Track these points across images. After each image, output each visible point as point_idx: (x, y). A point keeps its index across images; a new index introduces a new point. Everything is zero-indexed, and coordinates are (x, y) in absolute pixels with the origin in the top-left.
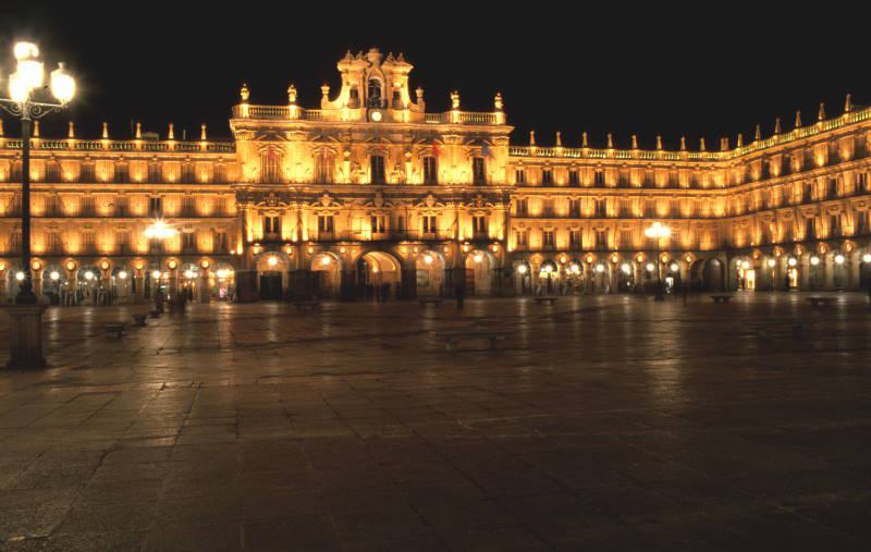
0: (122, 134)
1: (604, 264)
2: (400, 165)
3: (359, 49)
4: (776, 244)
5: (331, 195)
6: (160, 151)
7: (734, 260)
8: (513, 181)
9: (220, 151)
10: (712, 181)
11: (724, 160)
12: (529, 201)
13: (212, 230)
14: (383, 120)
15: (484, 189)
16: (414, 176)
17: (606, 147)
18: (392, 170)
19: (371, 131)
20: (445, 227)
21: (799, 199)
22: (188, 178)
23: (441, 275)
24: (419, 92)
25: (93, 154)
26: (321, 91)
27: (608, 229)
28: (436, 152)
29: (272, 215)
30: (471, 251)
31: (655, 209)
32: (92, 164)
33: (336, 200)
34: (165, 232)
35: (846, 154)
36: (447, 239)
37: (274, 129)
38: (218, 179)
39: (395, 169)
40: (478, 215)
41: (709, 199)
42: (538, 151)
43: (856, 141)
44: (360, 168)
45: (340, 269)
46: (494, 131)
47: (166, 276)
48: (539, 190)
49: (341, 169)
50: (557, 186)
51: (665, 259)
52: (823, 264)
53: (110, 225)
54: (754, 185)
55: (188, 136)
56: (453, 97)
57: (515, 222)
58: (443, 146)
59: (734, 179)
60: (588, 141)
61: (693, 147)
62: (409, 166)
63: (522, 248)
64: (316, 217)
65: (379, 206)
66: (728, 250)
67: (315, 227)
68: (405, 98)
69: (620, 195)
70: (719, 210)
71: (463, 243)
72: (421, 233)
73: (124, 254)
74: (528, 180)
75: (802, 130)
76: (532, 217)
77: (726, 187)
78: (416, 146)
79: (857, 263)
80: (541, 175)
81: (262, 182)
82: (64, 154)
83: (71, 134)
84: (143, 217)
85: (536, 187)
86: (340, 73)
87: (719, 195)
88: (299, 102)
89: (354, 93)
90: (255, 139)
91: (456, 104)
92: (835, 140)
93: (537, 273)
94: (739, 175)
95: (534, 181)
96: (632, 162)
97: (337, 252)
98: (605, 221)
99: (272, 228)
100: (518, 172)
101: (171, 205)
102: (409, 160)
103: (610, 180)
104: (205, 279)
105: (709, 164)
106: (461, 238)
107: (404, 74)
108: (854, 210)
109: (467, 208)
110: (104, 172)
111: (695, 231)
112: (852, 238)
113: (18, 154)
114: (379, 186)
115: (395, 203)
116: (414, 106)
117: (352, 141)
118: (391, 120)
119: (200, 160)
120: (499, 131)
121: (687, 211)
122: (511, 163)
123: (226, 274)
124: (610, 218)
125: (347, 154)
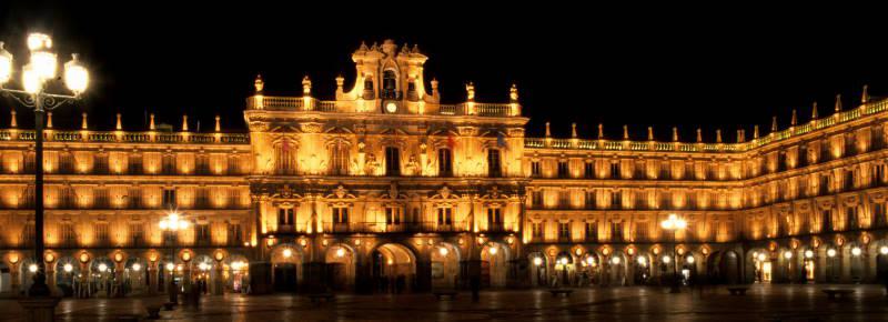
0: (135, 126)
1: (621, 257)
2: (415, 157)
3: (374, 40)
4: (792, 236)
5: (346, 187)
6: (174, 142)
7: (750, 252)
8: (528, 172)
9: (234, 143)
10: (728, 173)
11: (741, 152)
12: (545, 192)
13: (226, 222)
14: (397, 112)
15: (500, 181)
16: (429, 168)
17: (622, 139)
18: (407, 162)
19: (386, 122)
20: (460, 218)
21: (815, 191)
22: (202, 170)
23: (456, 267)
24: (434, 83)
25: (106, 146)
27: (623, 221)
28: (451, 144)
29: (287, 207)
30: (486, 243)
31: (671, 201)
32: (105, 155)
33: (350, 192)
34: (177, 223)
35: (863, 146)
36: (462, 231)
37: (289, 120)
38: (232, 171)
39: (410, 161)
40: (493, 207)
41: (725, 190)
42: (553, 143)
43: (873, 132)
45: (354, 261)
46: (510, 122)
47: (180, 268)
48: (554, 182)
49: (355, 161)
50: (573, 178)
51: (681, 251)
52: (840, 257)
53: (124, 218)
54: (770, 177)
55: (202, 128)
56: (468, 88)
57: (530, 214)
58: (458, 138)
59: (750, 171)
60: (604, 133)
61: (709, 138)
62: (424, 157)
63: (537, 240)
64: (331, 208)
65: (393, 198)
66: (745, 242)
67: (329, 219)
68: (420, 89)
69: (638, 187)
70: (736, 202)
71: (478, 235)
72: (436, 226)
73: (138, 246)
74: (543, 172)
75: (819, 122)
76: (547, 209)
77: (743, 179)
78: (431, 137)
79: (874, 256)
80: (556, 167)
81: (277, 174)
82: (78, 145)
83: (85, 126)
84: (157, 208)
85: (553, 178)
87: (735, 187)
88: (312, 94)
89: (369, 84)
90: (269, 130)
91: (471, 95)
92: (852, 132)
93: (552, 265)
94: (755, 166)
95: (549, 173)
96: (647, 154)
97: (352, 244)
98: (621, 213)
99: (287, 219)
100: (533, 164)
101: (185, 197)
102: (424, 152)
103: (626, 172)
104: (220, 271)
105: (726, 156)
106: (476, 230)
107: (419, 65)
108: (871, 201)
109: (483, 200)
110: (117, 164)
111: (711, 224)
112: (869, 230)
113: (31, 146)
114: (393, 178)
115: (410, 195)
116: (429, 98)
117: (366, 133)
118: (406, 111)
119: (214, 151)
120: (514, 122)
121: (703, 202)
122: (526, 155)
123: (240, 266)
124: (626, 210)
125: (362, 145)
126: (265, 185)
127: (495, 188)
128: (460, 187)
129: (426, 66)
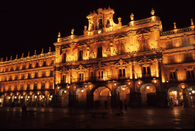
5: (82, 65)
16: (113, 52)
20: (129, 73)
24: (120, 19)
26: (84, 28)
39: (107, 51)
44: (93, 53)
46: (151, 25)
49: (87, 55)
55: (46, 51)
62: (112, 48)
86: (88, 20)
88: (75, 33)
91: (132, 19)
95: (177, 45)
99: (63, 79)
102: (112, 46)
106: (136, 78)
107: (111, 13)
125: (88, 48)
126: (58, 68)
127: (145, 57)
128: (128, 59)
129: (113, 15)
